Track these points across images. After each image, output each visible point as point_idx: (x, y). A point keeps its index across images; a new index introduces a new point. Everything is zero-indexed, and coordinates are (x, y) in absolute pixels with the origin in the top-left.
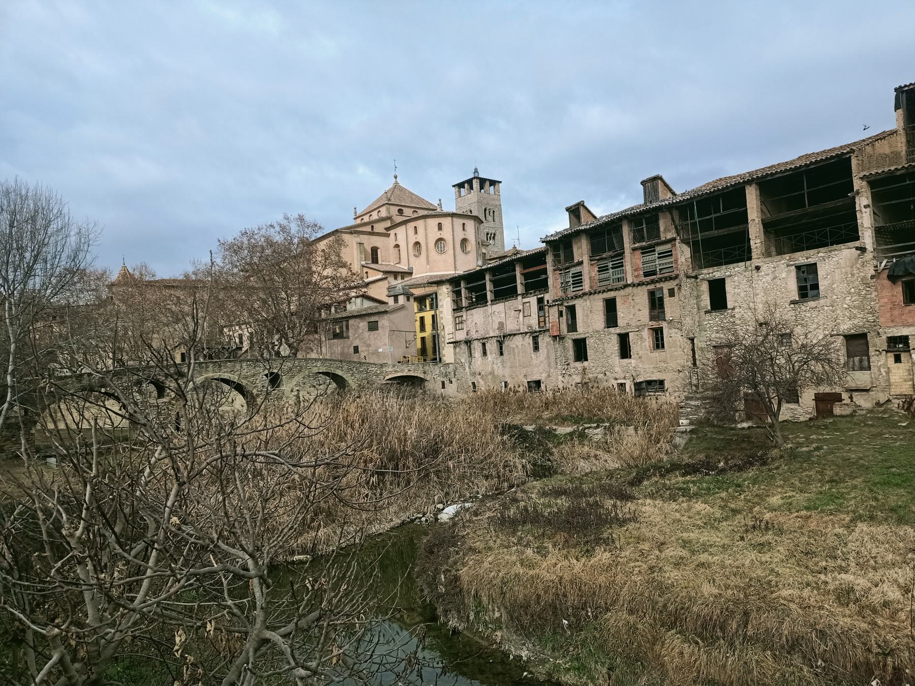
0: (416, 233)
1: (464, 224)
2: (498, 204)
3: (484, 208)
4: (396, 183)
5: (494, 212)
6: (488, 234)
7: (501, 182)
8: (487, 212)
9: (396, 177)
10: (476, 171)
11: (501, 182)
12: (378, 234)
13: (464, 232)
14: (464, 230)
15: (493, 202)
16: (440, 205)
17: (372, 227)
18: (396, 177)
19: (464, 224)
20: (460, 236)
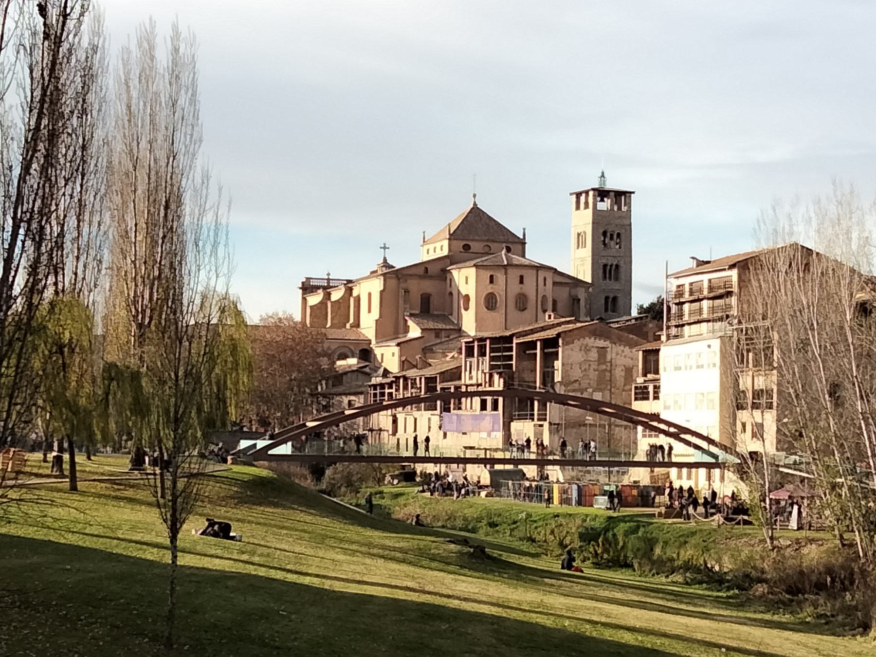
0: (467, 283)
1: (522, 277)
2: (626, 222)
3: (601, 231)
4: (475, 204)
5: (619, 235)
6: (605, 266)
7: (633, 193)
8: (608, 235)
9: (475, 196)
10: (603, 176)
11: (633, 193)
12: (431, 277)
13: (521, 286)
14: (521, 282)
15: (618, 222)
16: (524, 235)
17: (426, 269)
18: (475, 196)
19: (522, 277)
20: (515, 288)
